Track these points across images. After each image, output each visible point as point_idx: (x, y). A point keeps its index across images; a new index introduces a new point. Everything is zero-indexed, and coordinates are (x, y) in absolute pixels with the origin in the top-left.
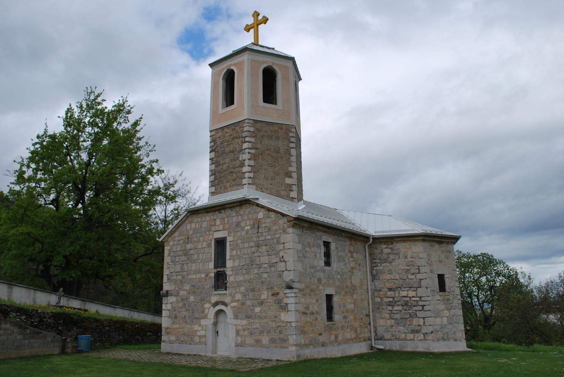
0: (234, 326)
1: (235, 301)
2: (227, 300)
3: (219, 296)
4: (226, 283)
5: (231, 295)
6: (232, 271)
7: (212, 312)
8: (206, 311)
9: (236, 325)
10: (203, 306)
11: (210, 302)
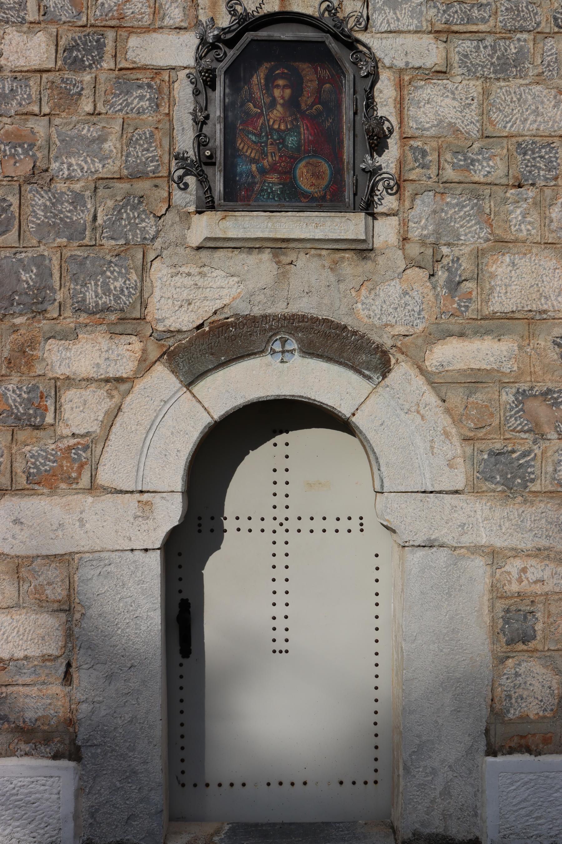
0: (478, 566)
1: (495, 324)
2: (385, 304)
3: (260, 269)
4: (377, 142)
5: (429, 260)
6: (444, 34)
7: (169, 421)
8: (80, 413)
9: (495, 556)
10: (23, 356)
11: (127, 319)
